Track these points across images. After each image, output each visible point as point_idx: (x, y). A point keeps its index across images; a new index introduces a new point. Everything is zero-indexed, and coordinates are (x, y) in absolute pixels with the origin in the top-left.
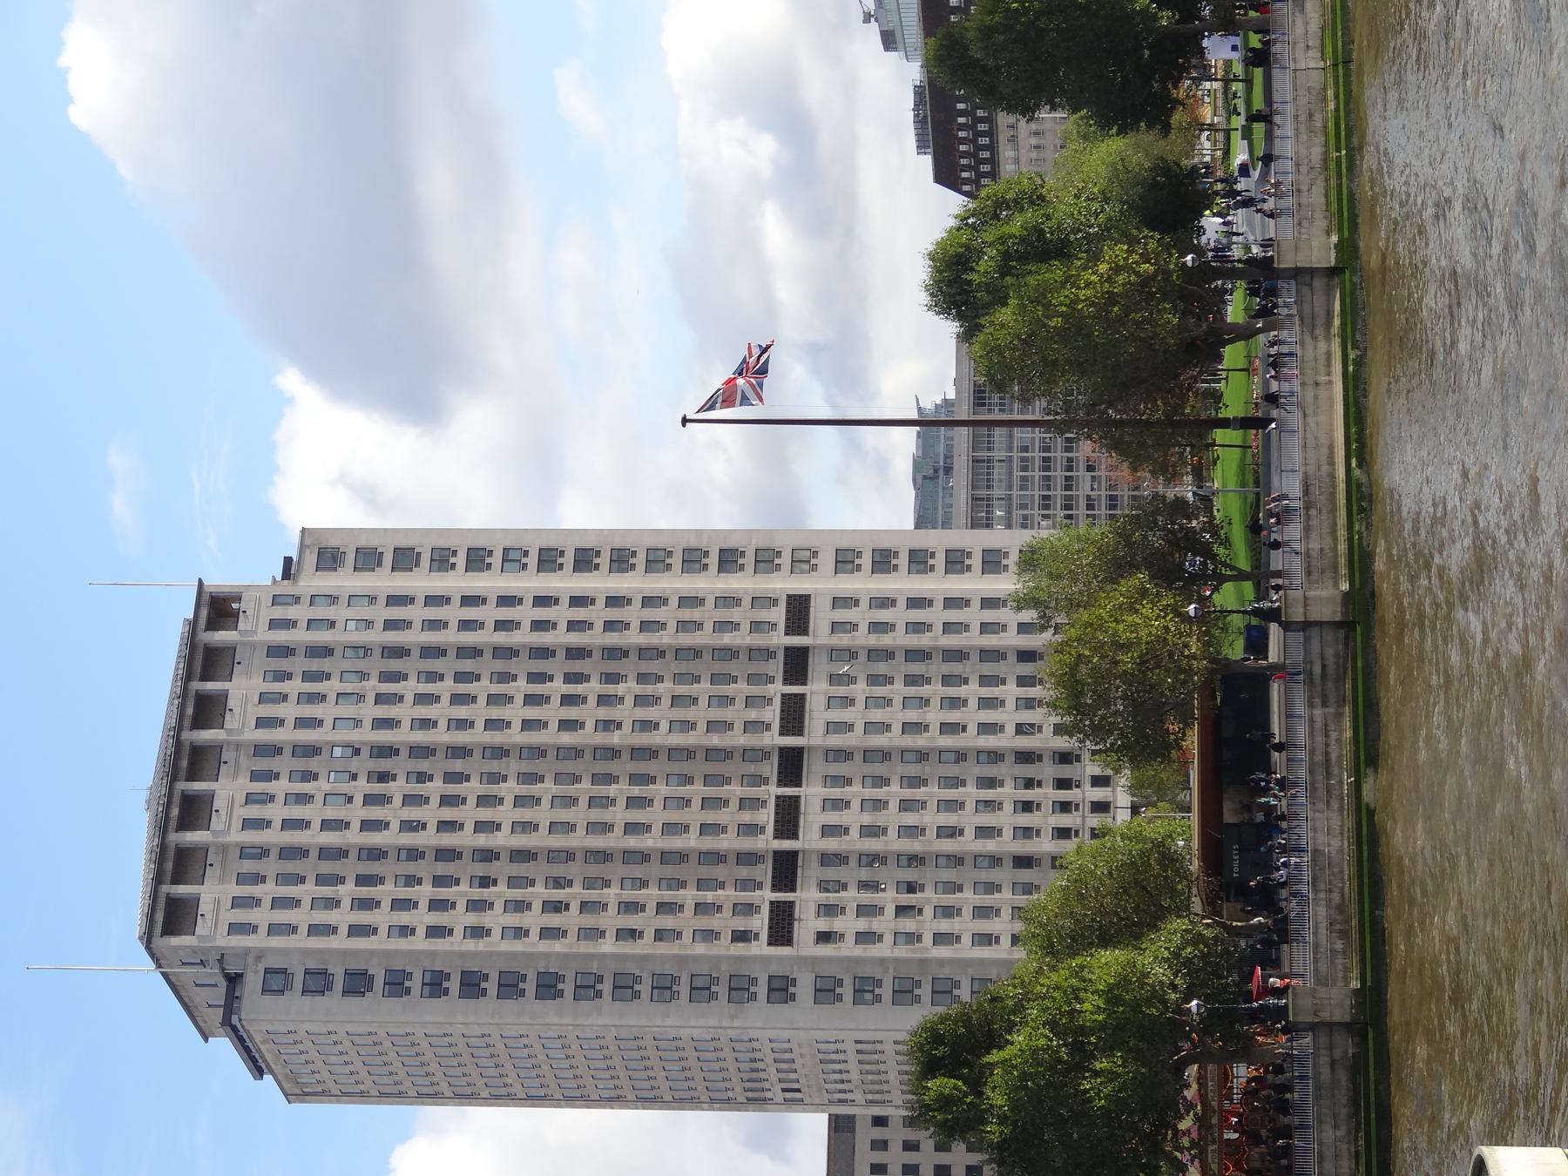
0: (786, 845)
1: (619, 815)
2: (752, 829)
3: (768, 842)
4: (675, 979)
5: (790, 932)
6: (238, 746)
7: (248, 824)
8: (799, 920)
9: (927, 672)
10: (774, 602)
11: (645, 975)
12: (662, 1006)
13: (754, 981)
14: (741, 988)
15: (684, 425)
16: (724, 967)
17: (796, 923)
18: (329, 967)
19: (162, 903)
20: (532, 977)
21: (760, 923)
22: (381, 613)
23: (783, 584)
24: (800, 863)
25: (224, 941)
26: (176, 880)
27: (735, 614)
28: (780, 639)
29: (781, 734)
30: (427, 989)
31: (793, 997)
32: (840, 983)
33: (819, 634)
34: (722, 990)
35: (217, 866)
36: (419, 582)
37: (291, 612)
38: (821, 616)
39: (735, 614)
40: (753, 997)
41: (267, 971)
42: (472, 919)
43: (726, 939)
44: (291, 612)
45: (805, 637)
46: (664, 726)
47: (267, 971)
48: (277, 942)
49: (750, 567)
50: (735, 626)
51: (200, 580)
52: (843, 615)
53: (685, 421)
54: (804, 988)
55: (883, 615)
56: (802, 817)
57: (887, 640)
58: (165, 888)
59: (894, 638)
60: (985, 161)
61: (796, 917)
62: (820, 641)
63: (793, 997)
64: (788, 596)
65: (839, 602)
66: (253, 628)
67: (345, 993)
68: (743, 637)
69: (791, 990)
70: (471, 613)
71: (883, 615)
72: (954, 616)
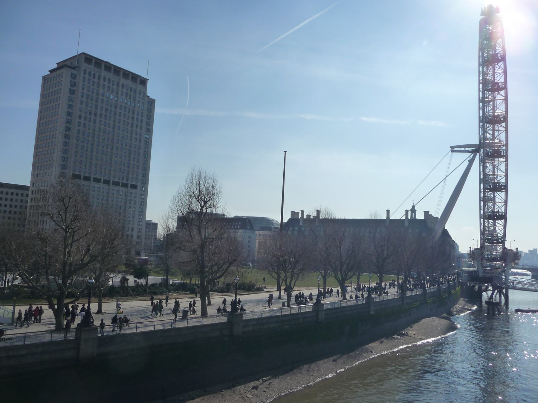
0: (92, 179)
7: (105, 78)
10: (136, 182)
14: (64, 167)
15: (284, 152)
20: (70, 126)
21: (77, 173)
23: (139, 185)
26: (95, 62)
28: (130, 183)
29: (113, 181)
33: (130, 190)
34: (64, 163)
38: (133, 191)
41: (76, 75)
47: (76, 75)
48: (82, 78)
51: (148, 80)
53: (285, 152)
55: (132, 202)
56: (97, 183)
57: (128, 202)
58: (94, 59)
60: (234, 227)
66: (140, 87)
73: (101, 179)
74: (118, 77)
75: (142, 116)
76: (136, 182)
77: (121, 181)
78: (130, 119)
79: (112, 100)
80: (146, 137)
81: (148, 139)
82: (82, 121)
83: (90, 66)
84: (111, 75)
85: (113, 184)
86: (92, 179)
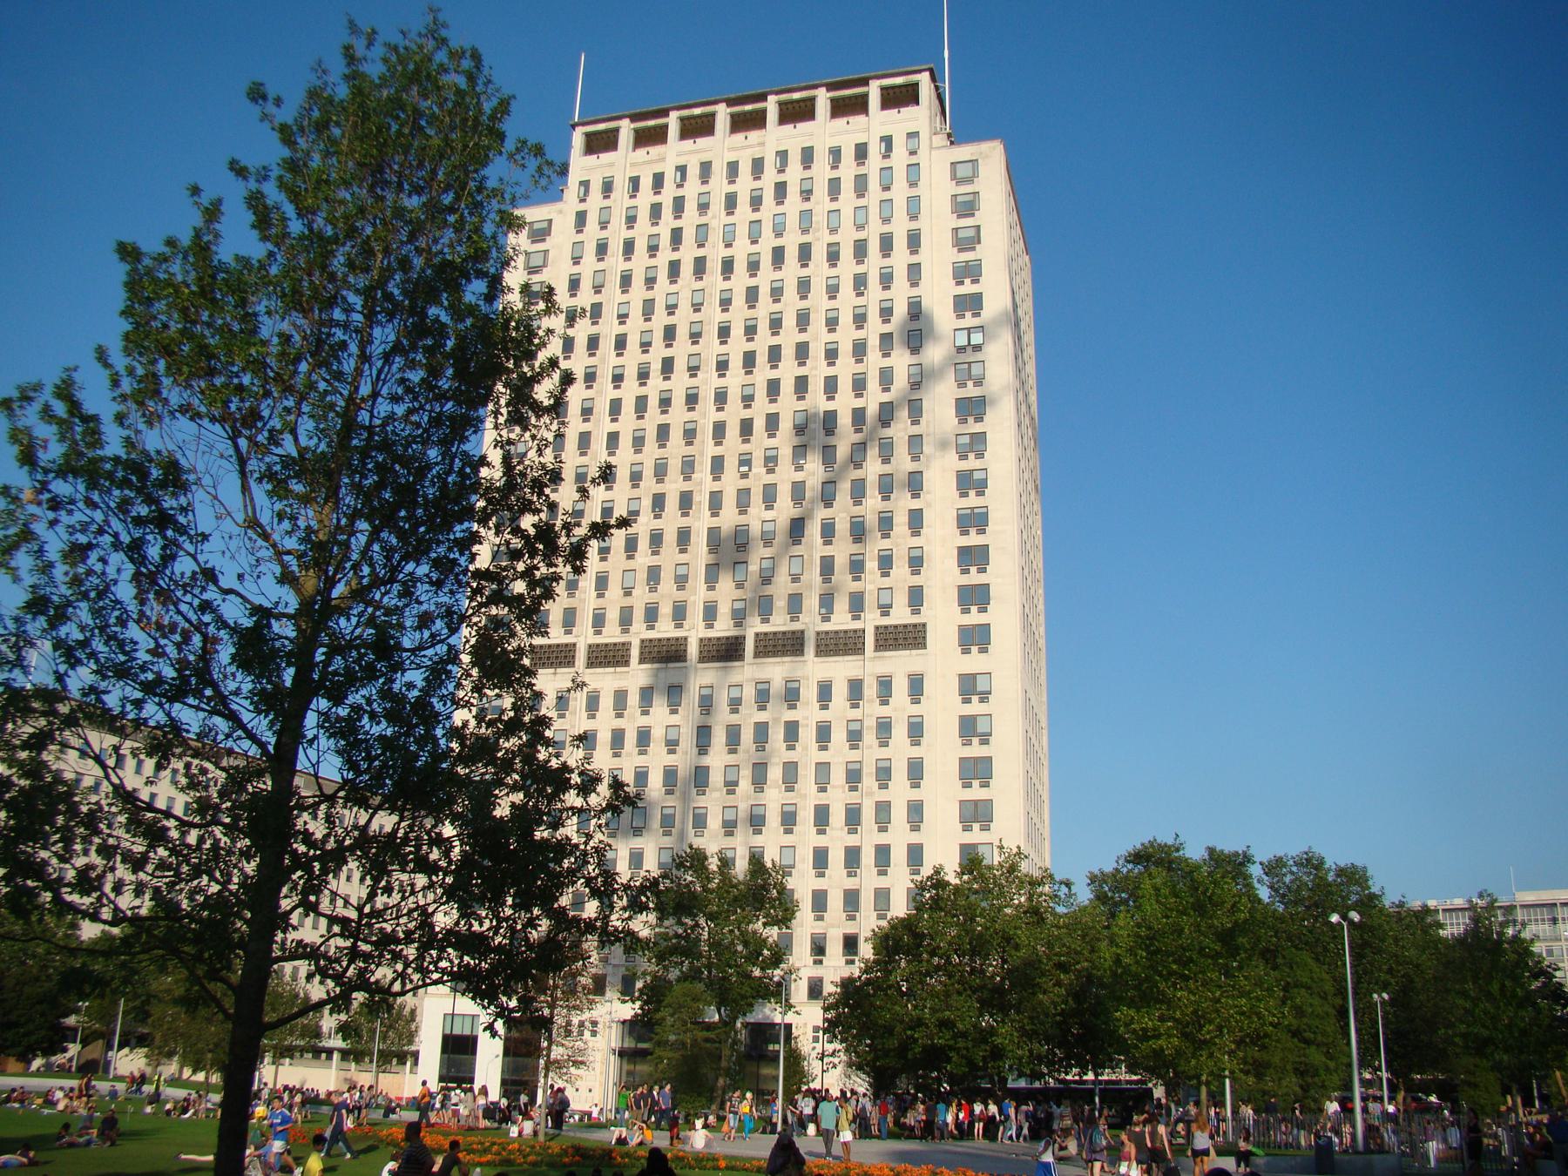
0: (635, 653)
1: (674, 486)
2: (651, 615)
6: (762, 144)
9: (834, 787)
10: (916, 612)
17: (552, 670)
22: (900, 228)
23: (943, 617)
24: (618, 669)
25: (574, 177)
27: (900, 569)
35: (647, 158)
38: (900, 664)
39: (900, 569)
41: (550, 221)
45: (873, 649)
49: (966, 580)
52: (900, 688)
55: (900, 732)
59: (870, 747)
61: (559, 670)
64: (924, 625)
65: (916, 686)
71: (900, 732)
72: (899, 814)
76: (916, 612)
77: (810, 622)
81: (977, 348)
85: (757, 655)
86: (635, 653)
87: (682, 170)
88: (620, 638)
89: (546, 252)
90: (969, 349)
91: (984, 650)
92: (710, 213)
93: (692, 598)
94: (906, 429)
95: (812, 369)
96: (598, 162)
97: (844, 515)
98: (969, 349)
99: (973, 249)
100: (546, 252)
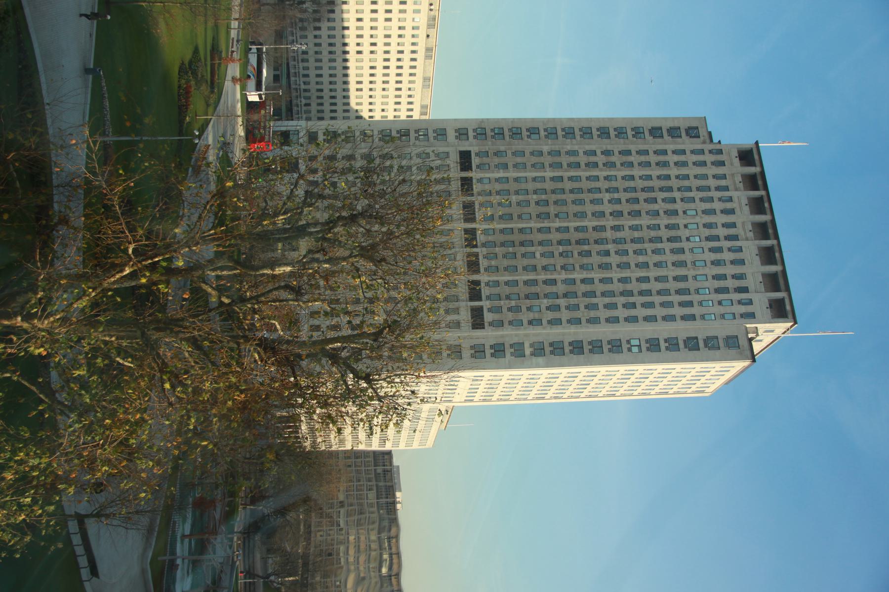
1: (552, 209)
3: (478, 200)
4: (511, 137)
5: (461, 158)
6: (747, 239)
7: (730, 199)
8: (457, 163)
10: (491, 324)
11: (526, 138)
12: (516, 126)
13: (475, 137)
16: (490, 143)
18: (671, 139)
19: (757, 162)
21: (475, 161)
22: (696, 310)
23: (488, 336)
30: (625, 131)
31: (456, 131)
32: (435, 138)
35: (737, 182)
36: (681, 330)
37: (743, 309)
39: (510, 316)
40: (474, 130)
41: (699, 137)
42: (613, 159)
43: (491, 153)
44: (743, 309)
46: (538, 255)
48: (699, 147)
50: (510, 309)
54: (451, 135)
61: (459, 164)
62: (464, 304)
63: (456, 131)
64: (484, 328)
65: (457, 325)
66: (761, 299)
67: (660, 128)
68: (505, 304)
69: (457, 134)
70: (649, 312)
73: (477, 271)
74: (751, 235)
75: (683, 318)
76: (491, 324)
78: (660, 286)
79: (686, 226)
80: (634, 342)
81: (629, 350)
82: (600, 159)
83: (737, 161)
84: (745, 218)
87: (730, 199)
88: (475, 191)
89: (681, 137)
90: (629, 346)
91: (473, 356)
92: (703, 215)
93: (495, 223)
94: (584, 316)
95: (615, 271)
96: (734, 157)
97: (539, 289)
98: (629, 346)
99: (686, 347)
100: (681, 137)
